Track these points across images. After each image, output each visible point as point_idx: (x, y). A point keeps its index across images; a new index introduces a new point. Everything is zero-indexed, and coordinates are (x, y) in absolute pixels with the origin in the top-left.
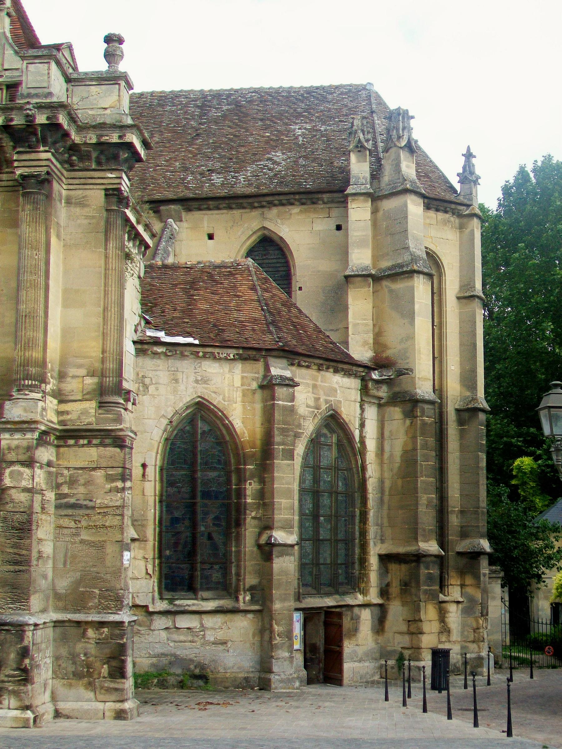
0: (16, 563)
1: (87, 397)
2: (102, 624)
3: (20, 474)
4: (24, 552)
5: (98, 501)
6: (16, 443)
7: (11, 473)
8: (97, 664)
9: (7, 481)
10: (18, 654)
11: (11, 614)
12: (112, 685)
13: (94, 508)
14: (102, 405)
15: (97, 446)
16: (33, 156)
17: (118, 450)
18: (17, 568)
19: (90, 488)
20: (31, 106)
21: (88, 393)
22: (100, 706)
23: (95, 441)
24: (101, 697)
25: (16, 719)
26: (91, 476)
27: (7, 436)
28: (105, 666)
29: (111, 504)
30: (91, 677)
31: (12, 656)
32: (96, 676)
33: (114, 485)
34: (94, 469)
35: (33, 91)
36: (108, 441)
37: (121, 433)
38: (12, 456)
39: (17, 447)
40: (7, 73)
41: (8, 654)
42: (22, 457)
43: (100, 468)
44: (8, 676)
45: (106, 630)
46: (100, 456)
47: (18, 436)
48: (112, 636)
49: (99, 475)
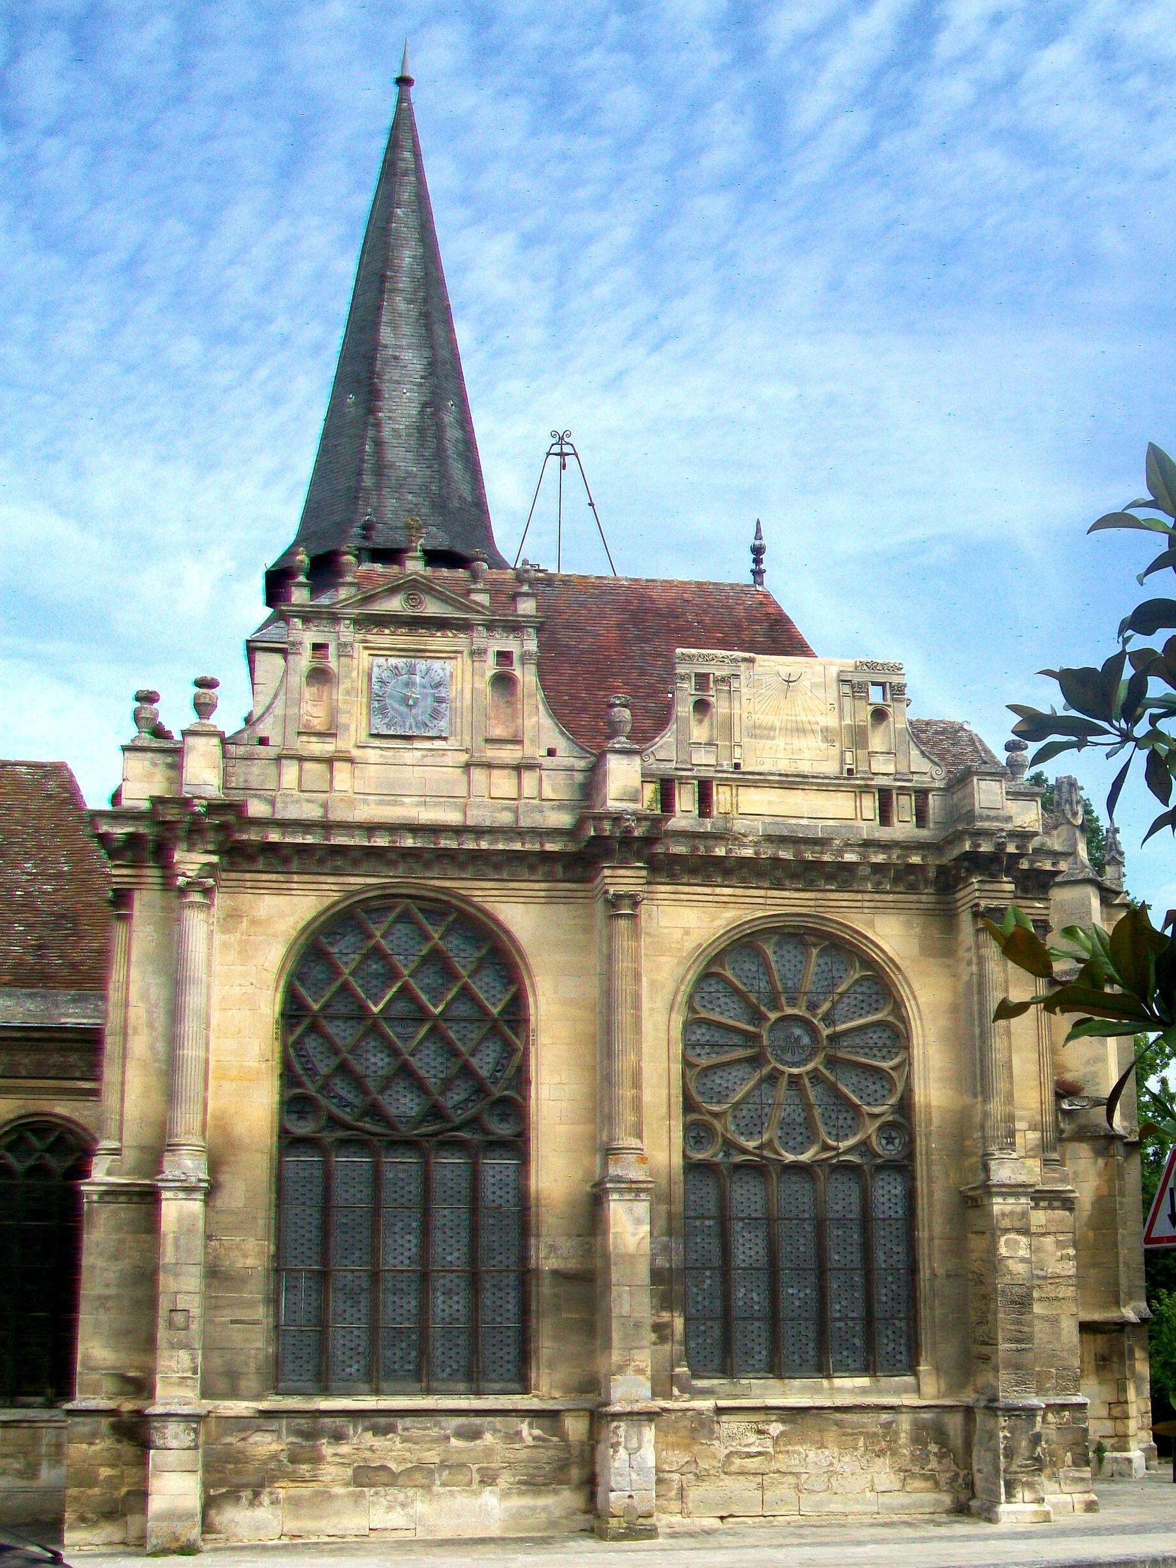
0: (1018, 1341)
1: (1030, 1153)
2: (1064, 1407)
3: (1017, 1242)
4: (1026, 1329)
5: (1050, 1270)
6: (1008, 1208)
7: (1007, 1241)
8: (1061, 1452)
9: (1003, 1251)
10: (1030, 1441)
11: (1016, 1398)
12: (1077, 1475)
13: (1045, 1278)
14: (1046, 1162)
15: (1045, 1208)
16: (996, 886)
17: (1067, 1213)
18: (1019, 1346)
19: (1040, 1255)
20: (1004, 834)
21: (1032, 1149)
22: (1068, 1498)
23: (1042, 1204)
24: (1066, 1489)
25: (1036, 1513)
26: (1040, 1242)
27: (999, 1200)
28: (1069, 1454)
29: (1063, 1273)
30: (1055, 1466)
31: (1024, 1443)
32: (1059, 1465)
33: (1064, 1252)
34: (1043, 1235)
35: (986, 812)
36: (1056, 1204)
37: (1072, 1195)
38: (1006, 1223)
39: (1012, 1213)
40: (915, 777)
41: (1019, 1442)
42: (1017, 1224)
43: (1049, 1233)
44: (1021, 1466)
45: (1067, 1413)
46: (1048, 1221)
47: (1011, 1200)
48: (1075, 1420)
49: (1049, 1240)
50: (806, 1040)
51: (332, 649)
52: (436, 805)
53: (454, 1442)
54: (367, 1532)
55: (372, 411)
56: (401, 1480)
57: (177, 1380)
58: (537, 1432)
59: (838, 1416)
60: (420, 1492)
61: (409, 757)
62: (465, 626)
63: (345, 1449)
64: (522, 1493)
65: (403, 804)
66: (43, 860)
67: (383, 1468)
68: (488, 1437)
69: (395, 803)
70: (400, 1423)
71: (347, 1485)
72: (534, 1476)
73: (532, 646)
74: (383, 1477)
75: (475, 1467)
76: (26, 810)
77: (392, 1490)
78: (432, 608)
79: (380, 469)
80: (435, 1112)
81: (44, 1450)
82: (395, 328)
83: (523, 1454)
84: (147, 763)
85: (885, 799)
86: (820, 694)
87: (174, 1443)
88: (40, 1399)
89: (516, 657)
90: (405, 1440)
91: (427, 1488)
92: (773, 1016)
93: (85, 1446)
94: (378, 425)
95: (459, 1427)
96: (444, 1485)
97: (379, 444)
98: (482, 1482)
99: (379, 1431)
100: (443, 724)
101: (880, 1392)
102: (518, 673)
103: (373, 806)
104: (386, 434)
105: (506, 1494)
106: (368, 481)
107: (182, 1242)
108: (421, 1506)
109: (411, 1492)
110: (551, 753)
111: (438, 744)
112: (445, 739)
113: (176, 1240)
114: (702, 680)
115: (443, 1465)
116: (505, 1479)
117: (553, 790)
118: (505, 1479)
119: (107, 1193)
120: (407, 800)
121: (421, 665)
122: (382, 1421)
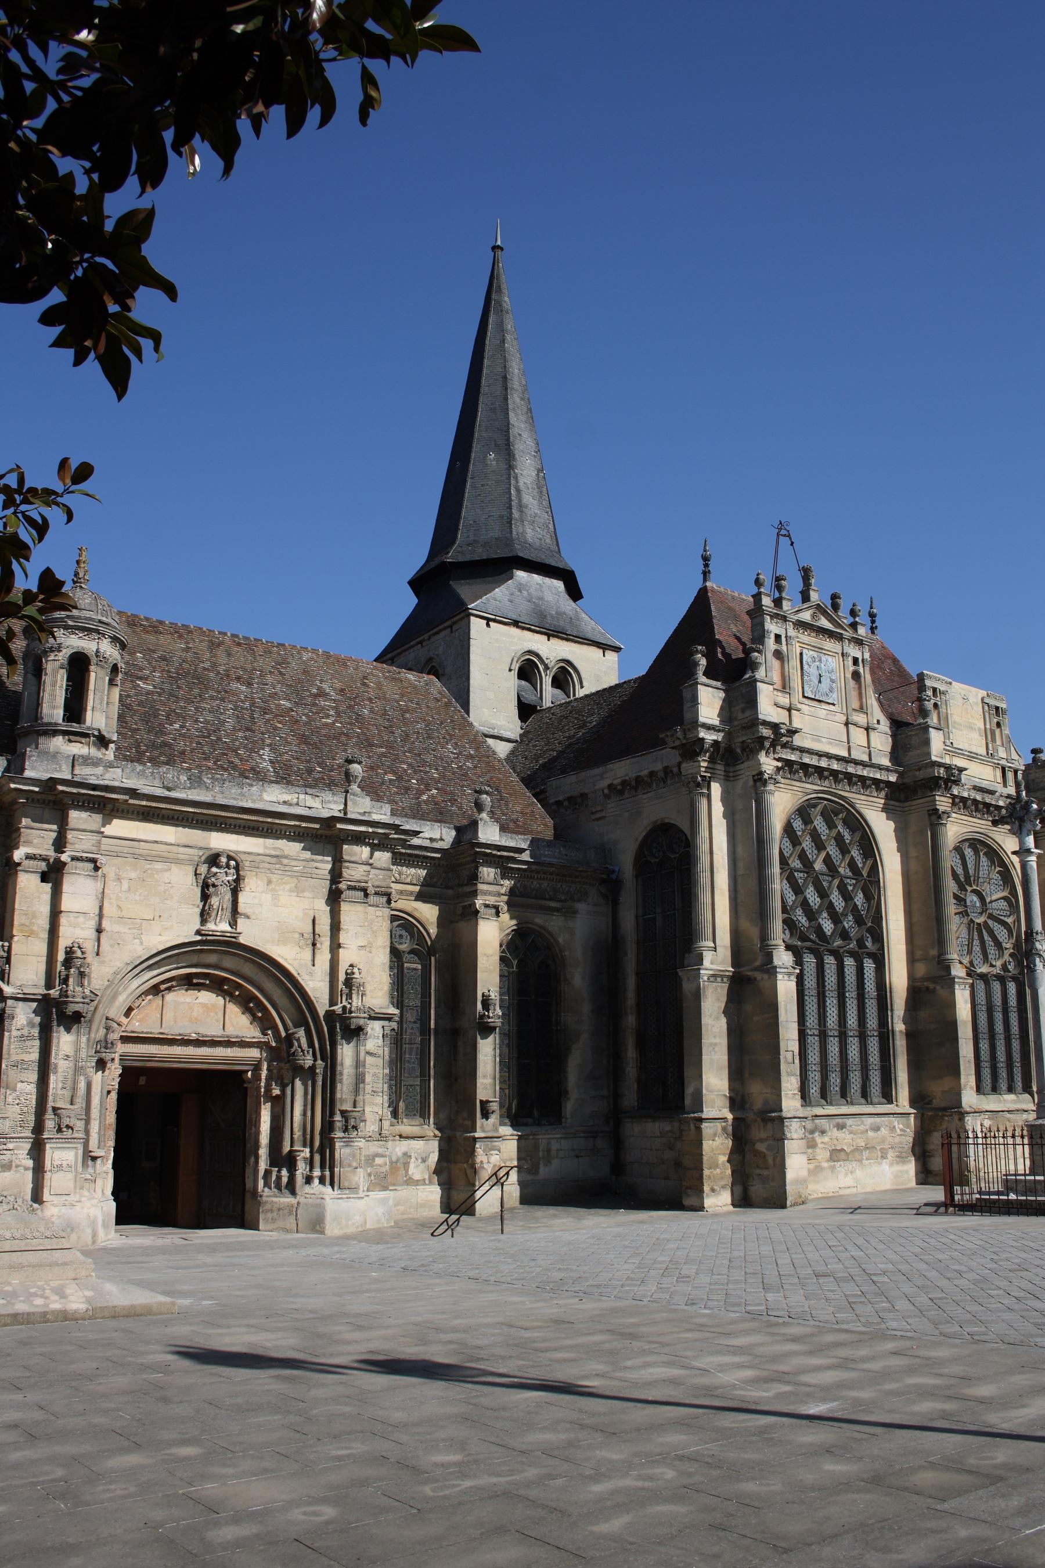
50: (978, 904)
51: (783, 639)
52: (837, 745)
53: (870, 1133)
54: (838, 1189)
55: (511, 467)
56: (850, 1157)
57: (791, 1096)
58: (901, 1126)
59: (1008, 1115)
60: (858, 1164)
61: (822, 713)
62: (839, 638)
63: (826, 1139)
64: (897, 1163)
65: (822, 742)
66: (456, 744)
67: (842, 1150)
68: (884, 1131)
69: (819, 741)
70: (850, 1122)
71: (828, 1161)
72: (901, 1153)
73: (867, 656)
74: (843, 1155)
75: (878, 1148)
76: (428, 707)
77: (847, 1163)
78: (824, 623)
79: (521, 507)
80: (845, 935)
81: (541, 1154)
82: (517, 415)
83: (897, 1140)
84: (710, 695)
85: (1003, 769)
86: (975, 708)
87: (795, 1136)
88: (530, 1120)
89: (860, 660)
90: (851, 1133)
91: (860, 1161)
92: (975, 887)
93: (711, 1142)
94: (516, 478)
95: (871, 1124)
96: (867, 1159)
97: (518, 490)
98: (882, 1157)
99: (841, 1127)
100: (835, 695)
101: (1020, 1102)
102: (861, 671)
103: (809, 740)
104: (521, 484)
105: (891, 1165)
106: (516, 514)
107: (788, 1007)
108: (859, 1173)
109: (854, 1164)
110: (878, 722)
111: (831, 708)
112: (833, 704)
113: (786, 1006)
114: (935, 690)
115: (866, 1148)
116: (891, 1154)
117: (881, 745)
118: (891, 1154)
119: (713, 976)
120: (824, 740)
121: (824, 658)
122: (840, 1121)
